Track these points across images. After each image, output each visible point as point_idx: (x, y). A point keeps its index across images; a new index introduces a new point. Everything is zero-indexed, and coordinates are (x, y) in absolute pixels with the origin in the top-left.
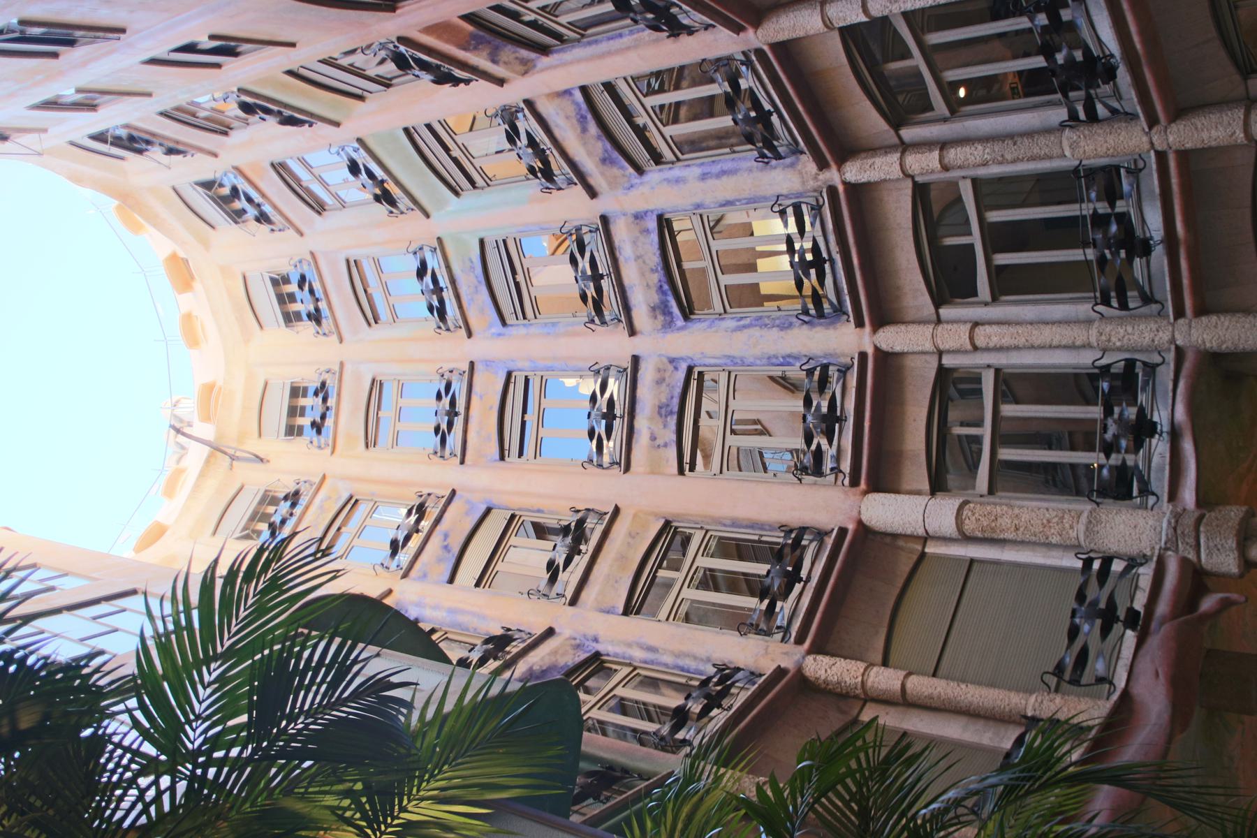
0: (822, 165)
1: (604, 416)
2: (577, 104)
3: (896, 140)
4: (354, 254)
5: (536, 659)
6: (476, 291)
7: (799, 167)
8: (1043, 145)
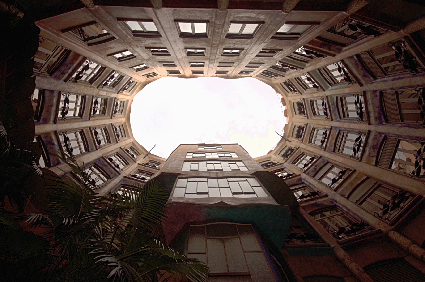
1: (357, 145)
2: (355, 60)
4: (312, 99)
5: (319, 201)
6: (334, 110)
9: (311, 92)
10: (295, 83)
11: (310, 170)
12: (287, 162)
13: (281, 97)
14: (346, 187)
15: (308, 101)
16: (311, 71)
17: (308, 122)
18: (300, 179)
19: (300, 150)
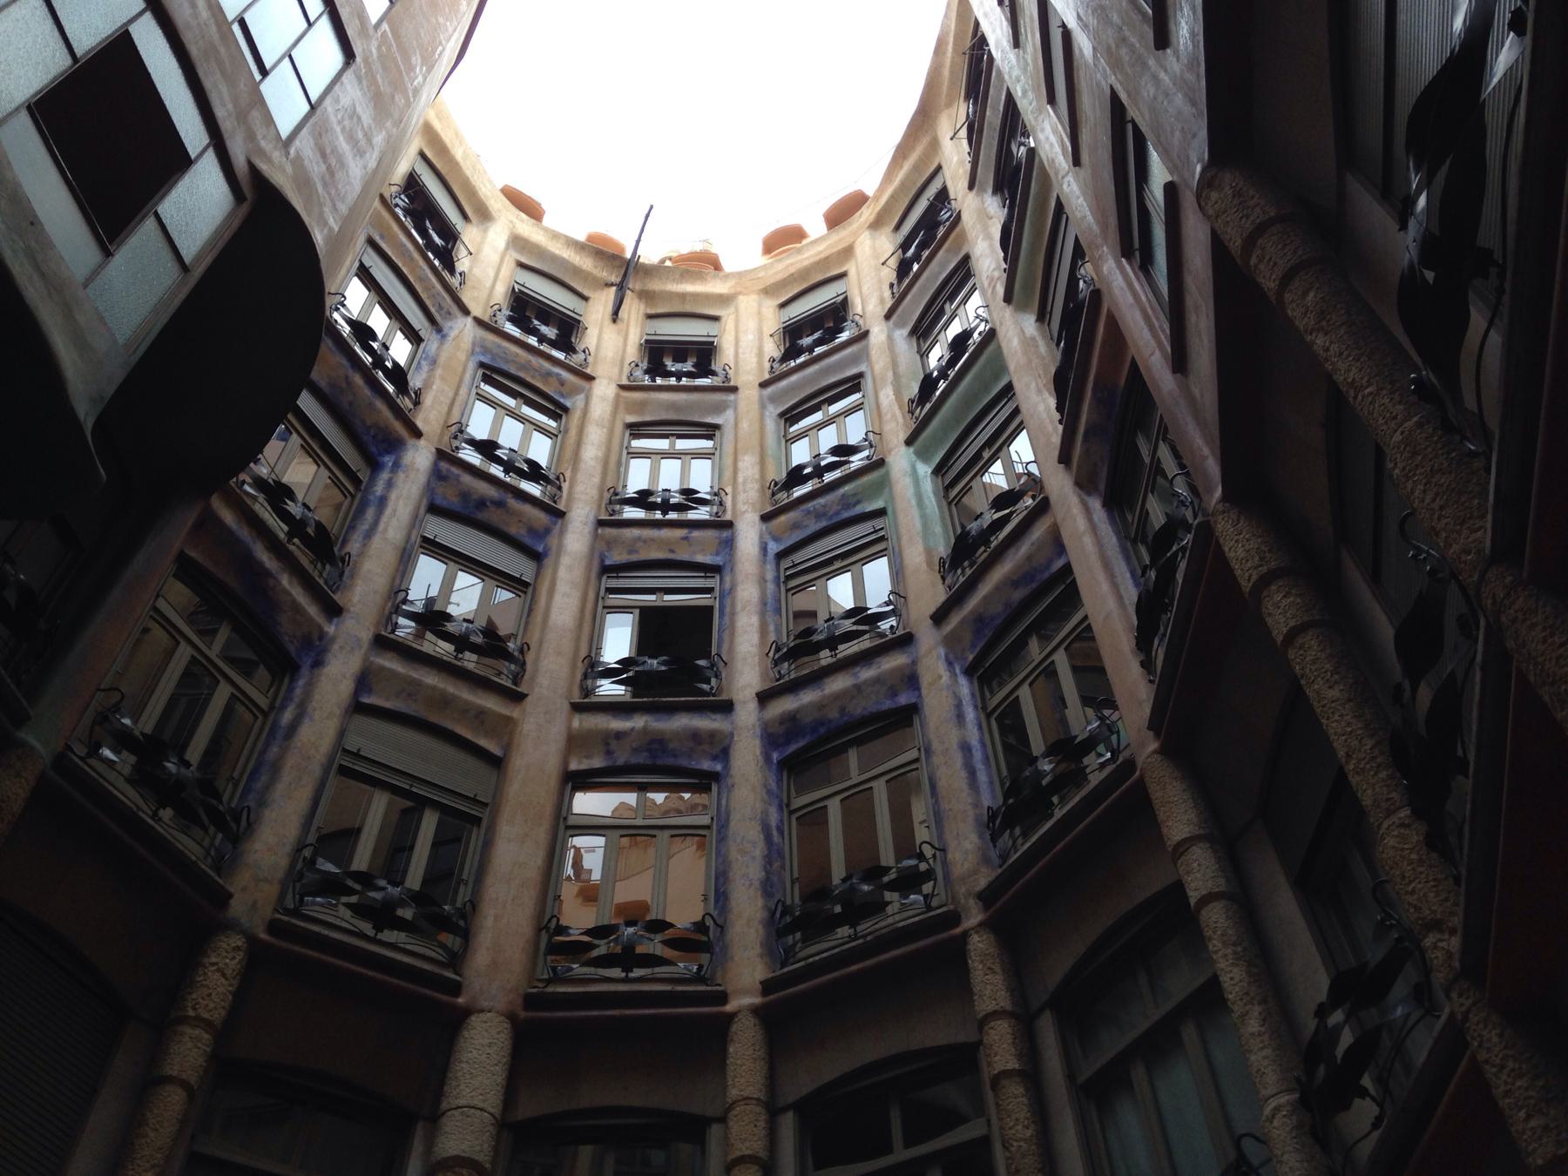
0: (986, 897)
2: (1050, 562)
4: (868, 383)
6: (819, 515)
9: (902, 369)
10: (943, 266)
11: (467, 479)
12: (481, 333)
13: (870, 192)
14: (418, 683)
15: (855, 360)
16: (999, 347)
17: (742, 394)
18: (394, 445)
19: (575, 391)
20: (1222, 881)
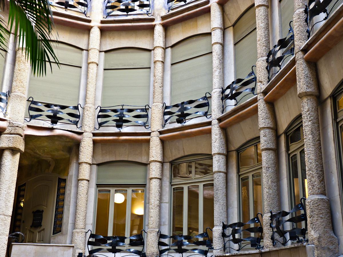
0: (163, 18)
3: (167, 46)
7: (164, 9)
8: (158, 97)
20: (220, 40)
